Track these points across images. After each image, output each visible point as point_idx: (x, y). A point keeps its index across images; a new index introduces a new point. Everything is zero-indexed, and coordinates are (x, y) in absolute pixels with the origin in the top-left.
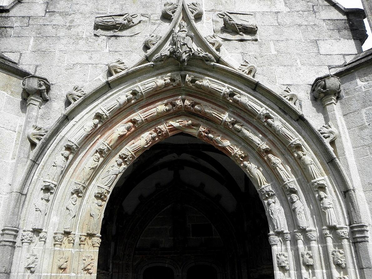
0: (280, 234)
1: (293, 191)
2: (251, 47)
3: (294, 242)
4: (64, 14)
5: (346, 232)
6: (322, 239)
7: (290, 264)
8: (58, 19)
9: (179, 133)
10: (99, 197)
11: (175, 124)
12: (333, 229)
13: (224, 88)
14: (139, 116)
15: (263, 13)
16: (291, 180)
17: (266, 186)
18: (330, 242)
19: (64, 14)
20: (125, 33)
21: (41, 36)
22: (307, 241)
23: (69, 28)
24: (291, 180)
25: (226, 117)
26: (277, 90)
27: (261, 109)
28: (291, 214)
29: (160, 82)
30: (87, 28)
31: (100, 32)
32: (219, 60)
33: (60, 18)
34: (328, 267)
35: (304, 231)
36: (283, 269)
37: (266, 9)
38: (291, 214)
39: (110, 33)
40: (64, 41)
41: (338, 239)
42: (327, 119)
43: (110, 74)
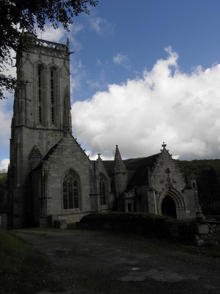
0: (177, 207)
1: (179, 203)
3: (179, 208)
5: (184, 207)
6: (181, 208)
7: (178, 210)
8: (156, 181)
9: (167, 195)
11: (167, 194)
12: (183, 207)
13: (173, 191)
17: (176, 202)
18: (182, 208)
19: (156, 180)
20: (163, 183)
21: (155, 184)
22: (180, 208)
23: (157, 182)
24: (179, 201)
26: (178, 191)
28: (178, 205)
30: (159, 182)
32: (174, 188)
33: (156, 180)
34: (182, 211)
35: (180, 207)
36: (177, 211)
38: (178, 205)
39: (162, 183)
40: (157, 184)
41: (183, 208)
42: (183, 195)
43: (163, 189)
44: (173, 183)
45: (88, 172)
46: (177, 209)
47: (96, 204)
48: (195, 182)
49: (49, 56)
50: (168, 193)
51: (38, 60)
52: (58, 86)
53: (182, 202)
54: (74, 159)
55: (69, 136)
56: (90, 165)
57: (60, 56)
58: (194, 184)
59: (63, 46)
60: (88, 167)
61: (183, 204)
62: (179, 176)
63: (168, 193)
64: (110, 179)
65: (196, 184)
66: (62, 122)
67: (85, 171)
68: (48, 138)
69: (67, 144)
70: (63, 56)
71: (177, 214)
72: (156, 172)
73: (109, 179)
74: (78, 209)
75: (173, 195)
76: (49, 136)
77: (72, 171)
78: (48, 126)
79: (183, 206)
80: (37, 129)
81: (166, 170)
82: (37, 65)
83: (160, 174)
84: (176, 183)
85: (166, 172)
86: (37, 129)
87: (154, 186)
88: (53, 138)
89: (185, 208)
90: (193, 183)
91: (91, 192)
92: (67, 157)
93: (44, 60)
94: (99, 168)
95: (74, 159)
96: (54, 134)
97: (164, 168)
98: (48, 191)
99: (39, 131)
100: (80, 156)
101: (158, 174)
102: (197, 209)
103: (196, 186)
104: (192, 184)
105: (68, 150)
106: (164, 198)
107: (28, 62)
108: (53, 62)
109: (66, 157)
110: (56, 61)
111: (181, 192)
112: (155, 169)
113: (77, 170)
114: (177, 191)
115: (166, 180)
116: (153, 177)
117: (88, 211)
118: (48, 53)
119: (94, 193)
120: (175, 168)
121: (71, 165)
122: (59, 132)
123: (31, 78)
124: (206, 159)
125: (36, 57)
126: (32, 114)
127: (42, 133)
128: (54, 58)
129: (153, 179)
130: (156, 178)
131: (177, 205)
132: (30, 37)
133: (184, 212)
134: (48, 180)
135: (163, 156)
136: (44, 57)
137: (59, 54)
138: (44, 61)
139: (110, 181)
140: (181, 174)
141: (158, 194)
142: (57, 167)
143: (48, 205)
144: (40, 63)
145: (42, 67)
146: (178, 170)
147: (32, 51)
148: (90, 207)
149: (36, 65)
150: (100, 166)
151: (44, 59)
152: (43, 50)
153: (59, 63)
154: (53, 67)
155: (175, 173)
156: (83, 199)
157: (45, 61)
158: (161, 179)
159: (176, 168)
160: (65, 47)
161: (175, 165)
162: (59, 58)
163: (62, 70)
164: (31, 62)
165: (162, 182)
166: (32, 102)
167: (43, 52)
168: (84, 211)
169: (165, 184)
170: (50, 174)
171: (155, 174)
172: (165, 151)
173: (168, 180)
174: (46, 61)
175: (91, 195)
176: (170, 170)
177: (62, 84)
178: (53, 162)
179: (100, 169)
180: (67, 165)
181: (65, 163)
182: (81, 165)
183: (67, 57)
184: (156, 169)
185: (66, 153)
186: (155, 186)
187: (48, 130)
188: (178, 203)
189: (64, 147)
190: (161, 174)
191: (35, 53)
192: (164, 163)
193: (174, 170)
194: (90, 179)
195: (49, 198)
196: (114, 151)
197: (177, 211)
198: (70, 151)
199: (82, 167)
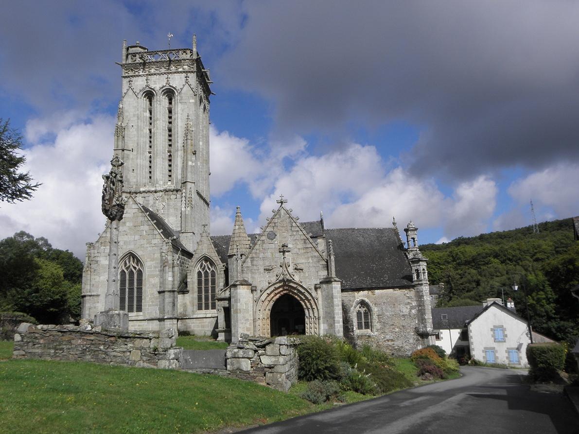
2: (302, 274)
4: (256, 266)
5: (317, 318)
8: (255, 268)
9: (285, 294)
10: (269, 310)
13: (295, 286)
14: (276, 292)
15: (306, 263)
16: (309, 306)
17: (305, 307)
19: (256, 266)
21: (252, 273)
23: (258, 270)
25: (296, 291)
27: (303, 291)
29: (281, 284)
30: (262, 270)
31: (265, 271)
32: (294, 280)
37: (306, 261)
44: (296, 271)
45: (158, 255)
46: (306, 320)
47: (164, 306)
50: (286, 290)
51: (144, 86)
52: (175, 119)
53: (313, 307)
54: (137, 237)
55: (131, 203)
56: (161, 245)
60: (159, 248)
61: (316, 310)
62: (312, 257)
63: (286, 290)
64: (224, 266)
66: (179, 177)
67: (154, 254)
68: (157, 205)
70: (186, 67)
71: (306, 329)
72: (258, 252)
73: (220, 266)
74: (141, 313)
75: (295, 293)
76: (157, 202)
77: (132, 255)
78: (157, 185)
79: (316, 314)
80: (140, 192)
81: (281, 247)
82: (143, 93)
83: (266, 254)
84: (301, 271)
85: (280, 252)
86: (140, 192)
87: (249, 278)
88: (164, 204)
89: (319, 319)
90: (416, 270)
91: (160, 287)
92: (126, 235)
93: (153, 83)
94: (203, 248)
95: (137, 237)
96: (166, 197)
97: (277, 242)
98: (91, 285)
99: (143, 195)
100: (146, 232)
101: (261, 255)
102: (423, 325)
105: (128, 224)
106: (277, 300)
107: (130, 92)
109: (123, 235)
110: (172, 78)
111: (313, 287)
112: (254, 247)
113: (139, 253)
114: (302, 286)
115: (279, 266)
116: (250, 261)
117: (153, 317)
118: (160, 70)
119: (162, 289)
120: (303, 242)
121: (131, 247)
122: (175, 192)
123: (134, 115)
124: (44, 237)
125: (143, 81)
126: (133, 170)
127: (147, 198)
128: (170, 76)
129: (249, 264)
130: (255, 263)
131: (306, 311)
132: (134, 53)
133: (317, 326)
134: (92, 270)
135: (276, 221)
137: (178, 67)
138: (154, 84)
139: (223, 270)
141: (259, 291)
144: (147, 89)
145: (151, 94)
147: (137, 73)
148: (158, 312)
149: (142, 93)
150: (205, 245)
151: (154, 82)
152: (152, 68)
154: (168, 90)
155: (303, 251)
156: (148, 299)
157: (156, 84)
158: (267, 264)
159: (305, 243)
161: (303, 237)
162: (178, 72)
163: (183, 92)
164: (134, 91)
165: (268, 270)
166: (135, 153)
167: (153, 71)
168: (148, 317)
169: (275, 273)
170: (97, 262)
171: (254, 255)
172: (282, 212)
173: (286, 266)
174: (157, 83)
175: (160, 292)
177: (181, 114)
179: (204, 250)
180: (125, 247)
182: (148, 245)
183: (192, 68)
184: (257, 247)
185: (125, 228)
186: (253, 278)
187: (156, 192)
188: (308, 309)
190: (269, 255)
191: (140, 76)
192: (278, 235)
193: (300, 246)
194: (161, 267)
196: (531, 202)
197: (306, 325)
198: (131, 224)
199: (149, 248)
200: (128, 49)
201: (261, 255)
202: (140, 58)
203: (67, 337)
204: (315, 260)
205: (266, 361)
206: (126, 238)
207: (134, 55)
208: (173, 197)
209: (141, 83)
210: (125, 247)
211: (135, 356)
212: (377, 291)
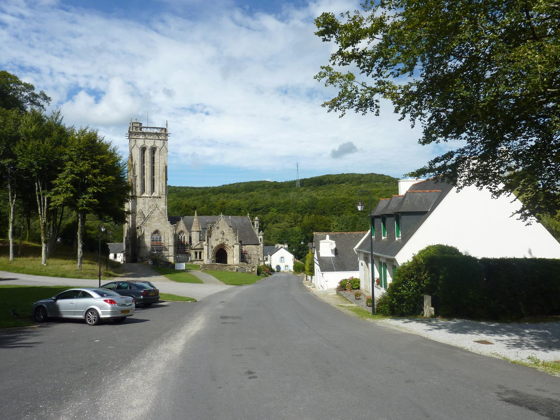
30: (214, 240)
48: (262, 238)
49: (151, 139)
57: (160, 138)
58: (261, 239)
59: (162, 129)
65: (262, 239)
69: (155, 215)
95: (160, 224)
103: (262, 241)
104: (260, 239)
105: (156, 218)
108: (154, 144)
125: (141, 141)
136: (146, 141)
140: (233, 235)
142: (148, 229)
143: (142, 251)
146: (231, 232)
147: (138, 137)
153: (159, 144)
160: (164, 129)
176: (224, 232)
178: (146, 226)
181: (153, 226)
185: (154, 220)
189: (153, 217)
190: (217, 234)
195: (142, 247)
196: (297, 164)
200: (133, 123)
201: (214, 235)
202: (140, 129)
203: (213, 266)
204: (232, 237)
205: (253, 270)
206: (155, 224)
207: (137, 127)
208: (157, 200)
209: (141, 142)
210: (154, 228)
211: (228, 269)
212: (246, 246)
